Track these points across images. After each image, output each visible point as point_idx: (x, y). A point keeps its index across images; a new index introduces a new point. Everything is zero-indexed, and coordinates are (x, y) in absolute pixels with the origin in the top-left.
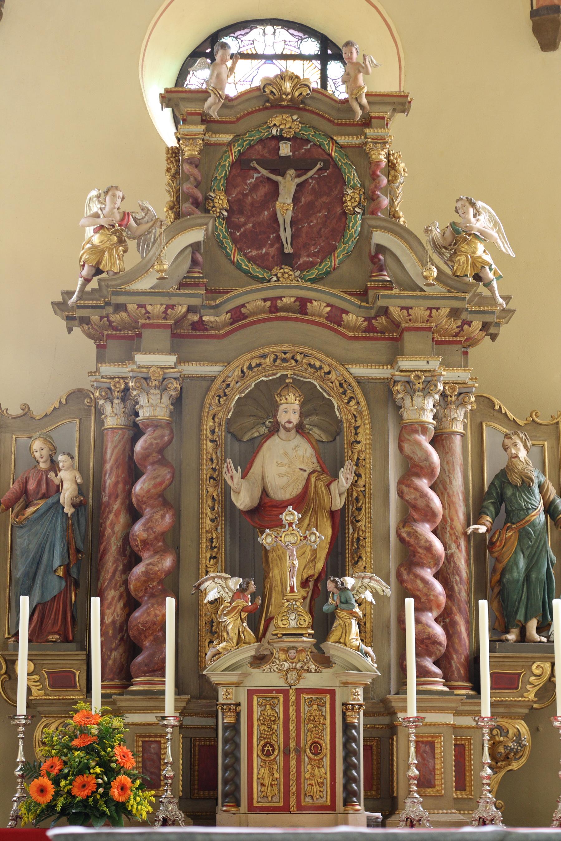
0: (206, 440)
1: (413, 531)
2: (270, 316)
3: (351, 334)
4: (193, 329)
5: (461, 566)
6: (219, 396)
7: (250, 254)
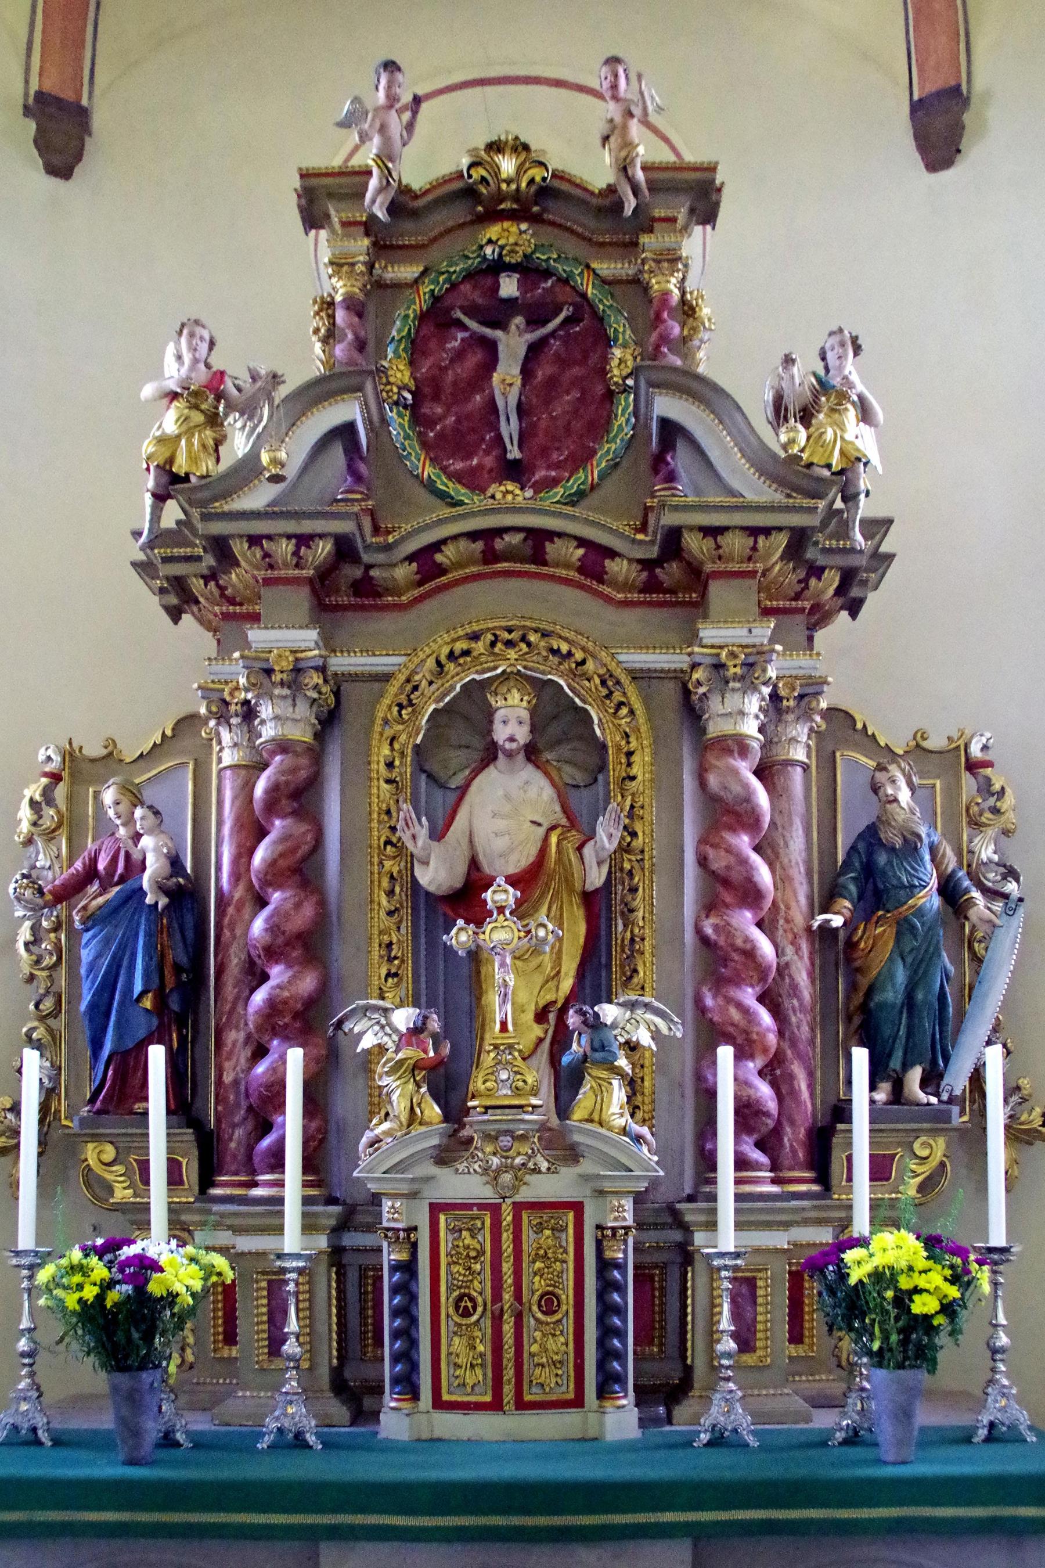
0: (378, 779)
1: (723, 923)
2: (487, 569)
3: (620, 596)
4: (357, 594)
5: (802, 983)
6: (401, 706)
7: (452, 468)
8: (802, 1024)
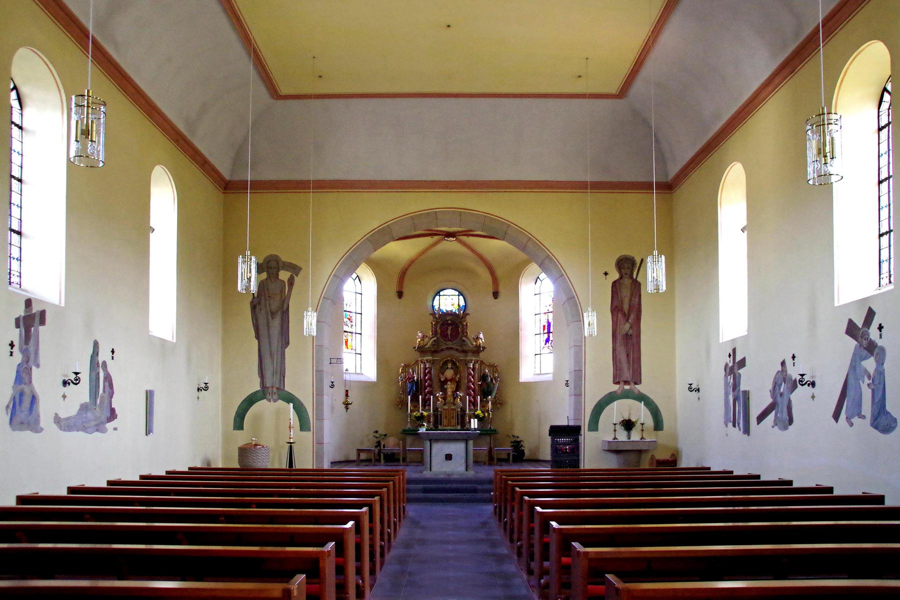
8: (477, 393)
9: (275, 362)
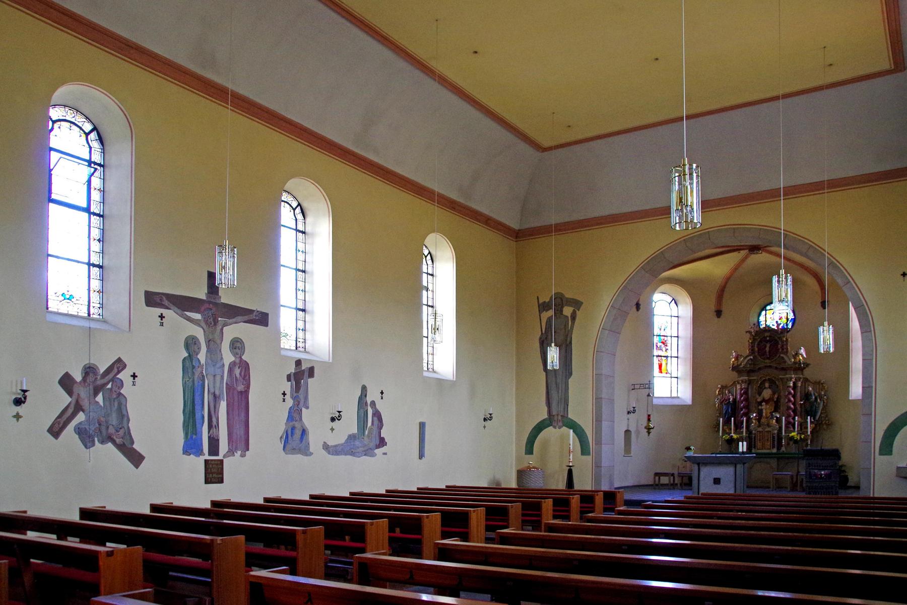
9: (560, 391)
